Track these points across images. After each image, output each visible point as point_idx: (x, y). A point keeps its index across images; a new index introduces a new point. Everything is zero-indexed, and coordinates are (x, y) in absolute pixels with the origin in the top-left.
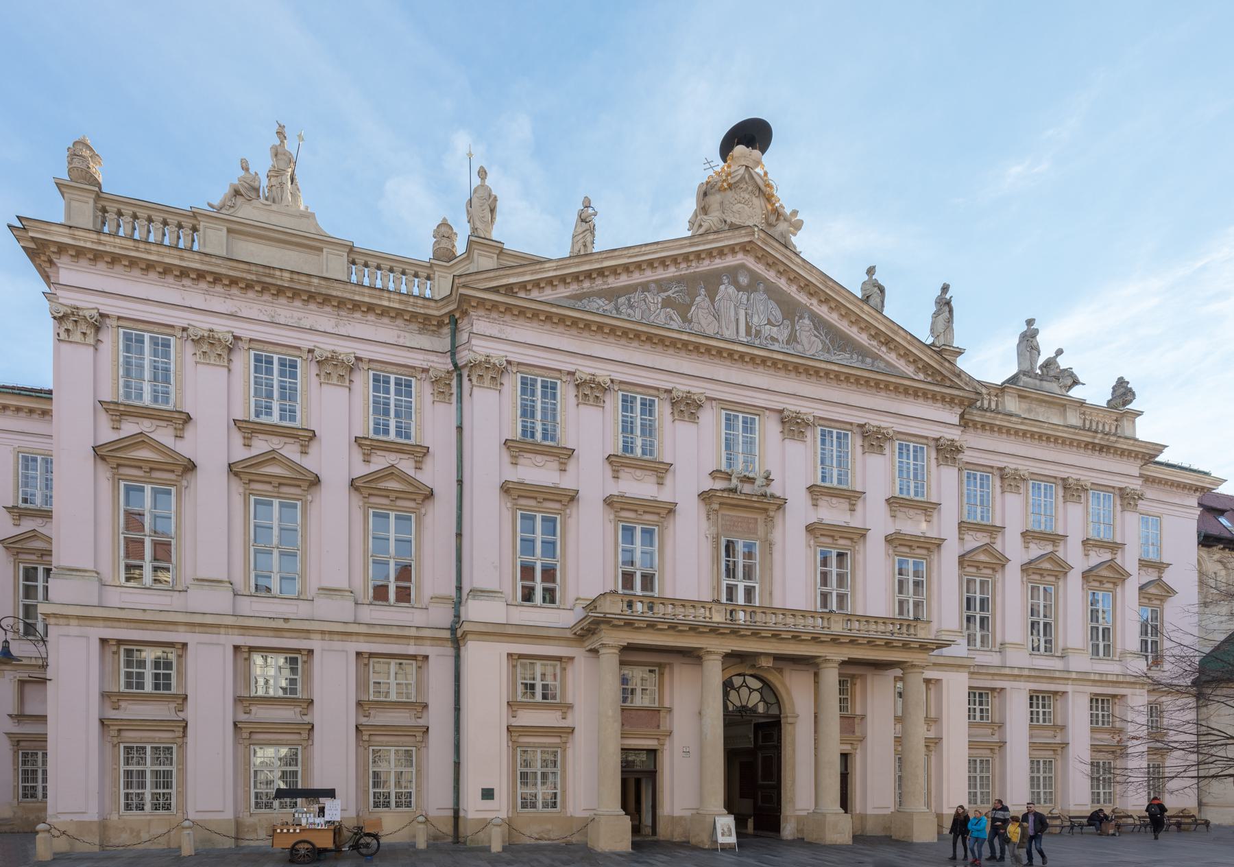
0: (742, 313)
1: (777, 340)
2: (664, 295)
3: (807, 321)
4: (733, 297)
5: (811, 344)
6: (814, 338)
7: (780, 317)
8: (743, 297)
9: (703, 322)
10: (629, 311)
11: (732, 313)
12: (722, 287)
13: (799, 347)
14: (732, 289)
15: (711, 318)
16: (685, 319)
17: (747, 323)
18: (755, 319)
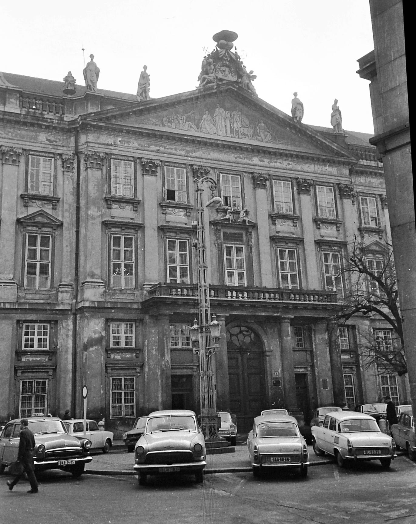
0: (228, 122)
1: (247, 135)
2: (186, 115)
3: (263, 125)
4: (223, 114)
5: (266, 136)
6: (266, 133)
7: (248, 123)
8: (228, 114)
9: (208, 129)
10: (169, 124)
11: (223, 123)
12: (217, 109)
13: (260, 138)
14: (222, 110)
15: (212, 125)
16: (198, 126)
17: (231, 127)
18: (235, 125)
